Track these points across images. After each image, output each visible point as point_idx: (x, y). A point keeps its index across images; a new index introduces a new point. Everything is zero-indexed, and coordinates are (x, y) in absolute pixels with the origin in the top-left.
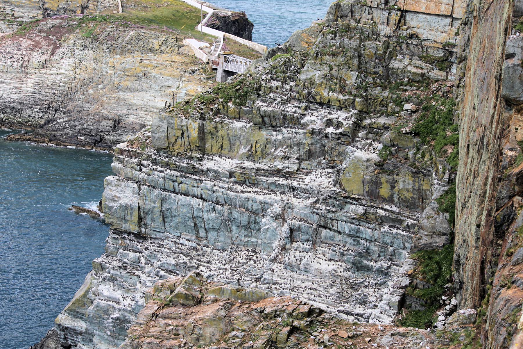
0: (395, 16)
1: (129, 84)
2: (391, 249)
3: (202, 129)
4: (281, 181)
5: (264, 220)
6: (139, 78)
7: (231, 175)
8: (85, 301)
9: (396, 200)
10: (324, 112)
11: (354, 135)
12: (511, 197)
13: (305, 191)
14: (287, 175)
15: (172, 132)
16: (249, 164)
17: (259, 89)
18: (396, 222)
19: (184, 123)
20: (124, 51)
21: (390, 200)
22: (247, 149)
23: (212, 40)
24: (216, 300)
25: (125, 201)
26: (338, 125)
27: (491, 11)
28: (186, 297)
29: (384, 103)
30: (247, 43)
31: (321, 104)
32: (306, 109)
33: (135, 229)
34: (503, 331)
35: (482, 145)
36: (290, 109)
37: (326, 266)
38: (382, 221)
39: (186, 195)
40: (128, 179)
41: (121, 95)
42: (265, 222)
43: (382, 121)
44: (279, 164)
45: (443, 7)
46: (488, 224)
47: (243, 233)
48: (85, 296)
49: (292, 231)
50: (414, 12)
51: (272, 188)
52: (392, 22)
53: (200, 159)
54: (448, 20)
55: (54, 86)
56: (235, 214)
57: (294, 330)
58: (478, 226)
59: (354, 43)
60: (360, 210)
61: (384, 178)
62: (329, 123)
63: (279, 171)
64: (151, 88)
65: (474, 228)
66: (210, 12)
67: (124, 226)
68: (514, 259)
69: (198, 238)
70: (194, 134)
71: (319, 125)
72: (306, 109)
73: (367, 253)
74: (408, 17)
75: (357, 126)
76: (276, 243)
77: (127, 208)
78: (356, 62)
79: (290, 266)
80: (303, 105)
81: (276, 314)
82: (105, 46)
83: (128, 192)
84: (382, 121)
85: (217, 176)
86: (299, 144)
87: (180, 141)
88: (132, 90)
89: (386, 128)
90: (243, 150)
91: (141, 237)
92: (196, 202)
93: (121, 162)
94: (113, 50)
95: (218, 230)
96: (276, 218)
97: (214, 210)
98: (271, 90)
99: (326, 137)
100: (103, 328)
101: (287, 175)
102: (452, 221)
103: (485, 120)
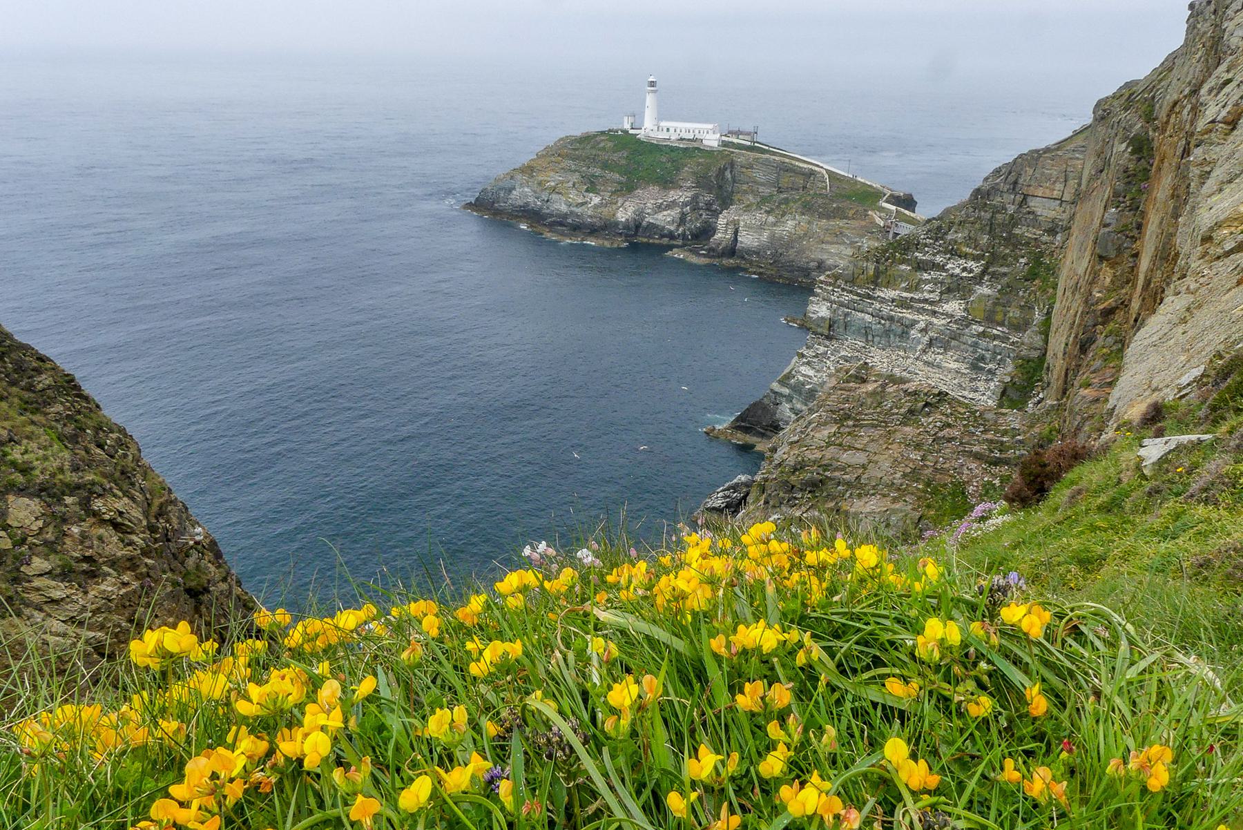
0: (1019, 198)
2: (999, 357)
3: (876, 269)
4: (927, 307)
5: (912, 332)
6: (837, 236)
7: (893, 300)
8: (789, 376)
9: (1006, 323)
10: (962, 261)
11: (982, 279)
12: (1095, 326)
13: (942, 314)
14: (932, 303)
15: (856, 271)
16: (905, 294)
17: (918, 244)
18: (1004, 339)
20: (828, 218)
21: (1002, 324)
23: (888, 212)
24: (876, 381)
25: (820, 315)
26: (971, 271)
27: (1095, 193)
28: (857, 377)
29: (1004, 257)
30: (912, 215)
31: (960, 256)
33: (826, 332)
34: (1079, 418)
35: (1076, 288)
36: (939, 259)
37: (954, 365)
38: (995, 337)
39: (862, 312)
40: (824, 300)
42: (914, 333)
43: (1005, 270)
44: (927, 296)
45: (1055, 192)
46: (1075, 343)
47: (898, 339)
48: (790, 372)
49: (931, 340)
50: (1033, 196)
51: (921, 311)
52: (1017, 203)
53: (874, 290)
54: (1059, 202)
55: (781, 238)
56: (893, 327)
57: (927, 405)
58: (1067, 345)
59: (988, 216)
60: (981, 329)
61: (999, 308)
62: (964, 269)
63: (927, 300)
65: (1063, 345)
67: (819, 330)
68: (1092, 369)
69: (867, 341)
70: (871, 272)
71: (957, 271)
72: (949, 259)
73: (982, 358)
74: (1029, 199)
75: (984, 273)
76: (920, 347)
77: (822, 318)
78: (988, 228)
79: (927, 363)
80: (948, 256)
81: (915, 393)
83: (824, 308)
84: (1005, 270)
85: (883, 301)
86: (941, 283)
87: (861, 276)
88: (832, 243)
89: (1005, 274)
90: (903, 285)
91: (829, 338)
92: (868, 318)
93: (821, 288)
94: (821, 216)
95: (881, 337)
96: (921, 331)
97: (880, 323)
98: (926, 245)
99: (961, 278)
100: (800, 394)
101: (932, 303)
102: (1046, 342)
103: (1081, 271)
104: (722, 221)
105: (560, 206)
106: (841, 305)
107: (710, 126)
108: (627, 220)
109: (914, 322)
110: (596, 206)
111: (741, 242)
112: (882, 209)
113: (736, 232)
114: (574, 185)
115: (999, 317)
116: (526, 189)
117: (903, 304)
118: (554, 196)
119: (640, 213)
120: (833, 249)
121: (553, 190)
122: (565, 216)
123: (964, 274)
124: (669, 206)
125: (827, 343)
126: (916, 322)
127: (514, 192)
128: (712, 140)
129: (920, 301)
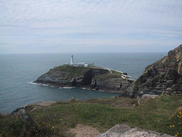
26: (171, 82)
36: (165, 80)
66: (123, 73)
104: (93, 80)
105: (57, 80)
106: (146, 91)
110: (65, 80)
112: (123, 76)
113: (96, 82)
115: (179, 90)
117: (159, 89)
118: (56, 78)
119: (75, 80)
120: (116, 83)
121: (55, 77)
124: (80, 79)
128: (86, 65)
129: (162, 88)
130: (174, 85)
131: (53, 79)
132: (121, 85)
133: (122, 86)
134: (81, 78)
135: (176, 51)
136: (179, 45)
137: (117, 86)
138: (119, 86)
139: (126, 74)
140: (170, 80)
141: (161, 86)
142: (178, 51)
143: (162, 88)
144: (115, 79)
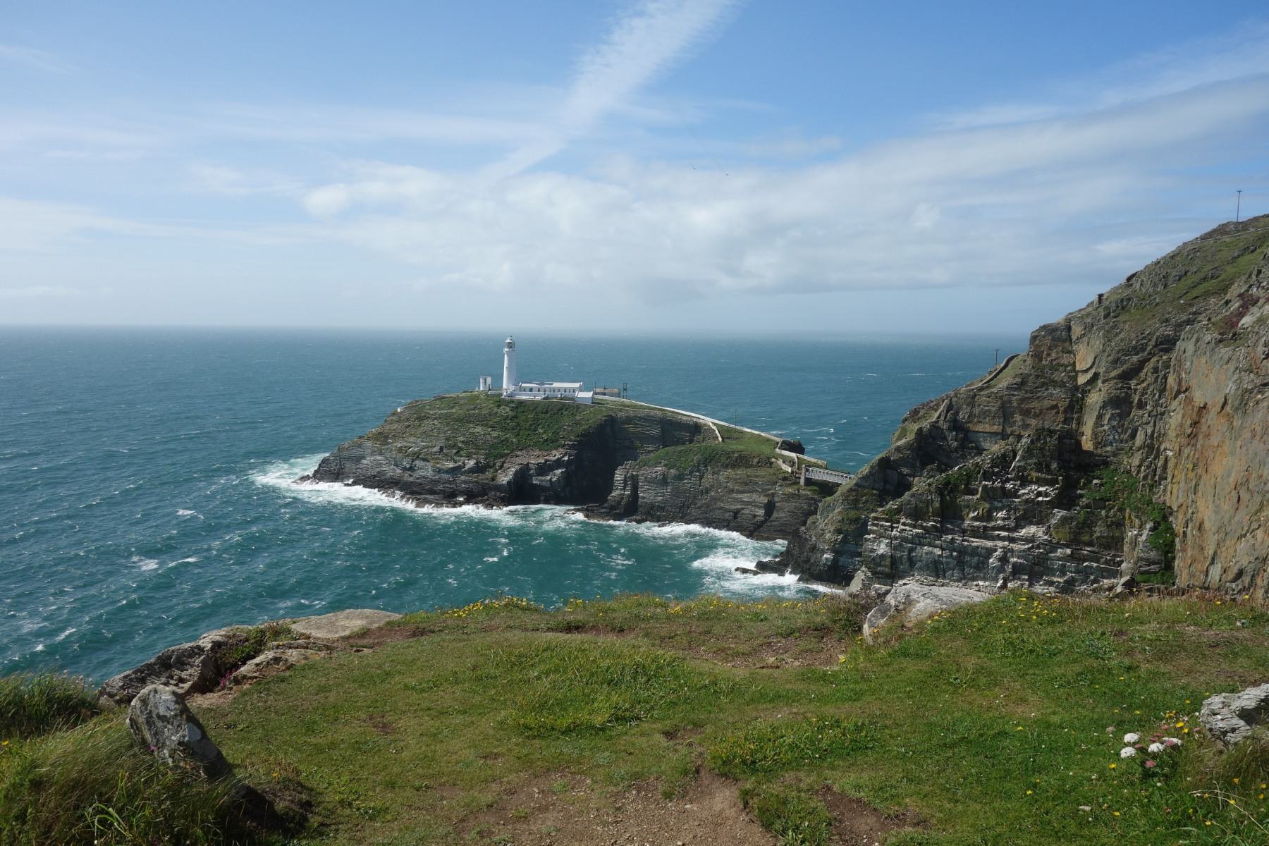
1: (741, 488)
4: (1004, 534)
6: (747, 484)
10: (1034, 487)
19: (929, 498)
20: (734, 466)
22: (976, 514)
25: (881, 552)
26: (1047, 495)
32: (1021, 486)
33: (887, 570)
36: (1009, 486)
41: (735, 495)
60: (1068, 551)
64: (756, 491)
66: (779, 440)
70: (937, 505)
77: (882, 556)
82: (719, 464)
83: (883, 546)
88: (743, 492)
104: (619, 476)
105: (426, 471)
106: (905, 539)
107: (577, 385)
108: (509, 482)
109: (990, 551)
110: (472, 471)
111: (643, 498)
113: (635, 489)
114: (441, 449)
115: (1086, 538)
116: (379, 458)
117: (975, 533)
118: (419, 463)
120: (745, 497)
121: (417, 456)
122: (436, 482)
123: (1040, 499)
125: (889, 581)
126: (990, 551)
127: (364, 461)
129: (995, 528)
130: (1059, 514)
131: (404, 469)
132: (770, 508)
133: (775, 515)
134: (558, 464)
135: (1077, 330)
136: (1094, 298)
137: (747, 511)
138: (761, 512)
139: (798, 448)
140: (1039, 482)
141: (988, 517)
142: (1088, 328)
143: (995, 528)
144: (741, 472)
